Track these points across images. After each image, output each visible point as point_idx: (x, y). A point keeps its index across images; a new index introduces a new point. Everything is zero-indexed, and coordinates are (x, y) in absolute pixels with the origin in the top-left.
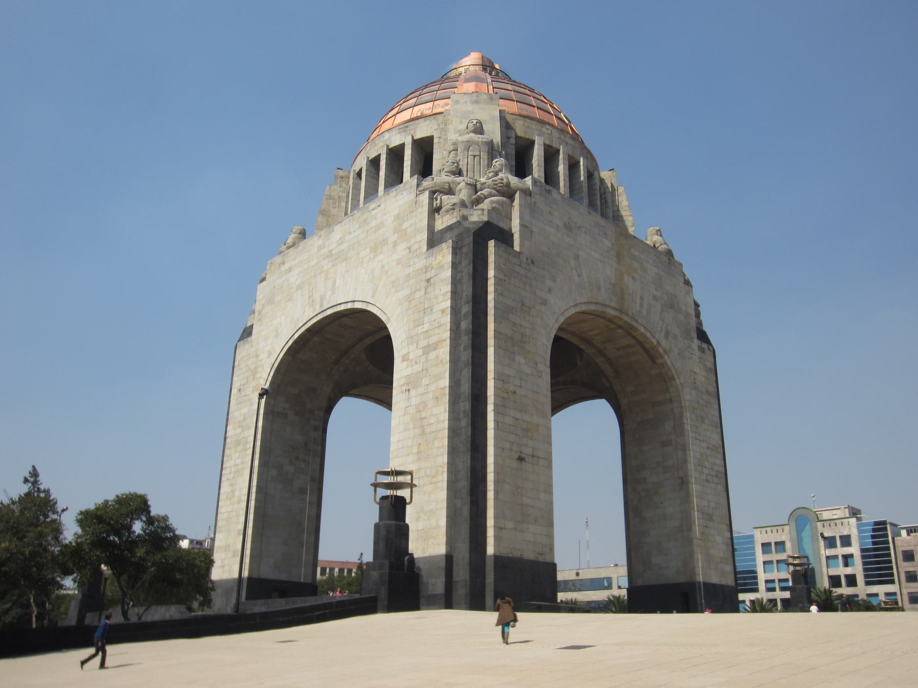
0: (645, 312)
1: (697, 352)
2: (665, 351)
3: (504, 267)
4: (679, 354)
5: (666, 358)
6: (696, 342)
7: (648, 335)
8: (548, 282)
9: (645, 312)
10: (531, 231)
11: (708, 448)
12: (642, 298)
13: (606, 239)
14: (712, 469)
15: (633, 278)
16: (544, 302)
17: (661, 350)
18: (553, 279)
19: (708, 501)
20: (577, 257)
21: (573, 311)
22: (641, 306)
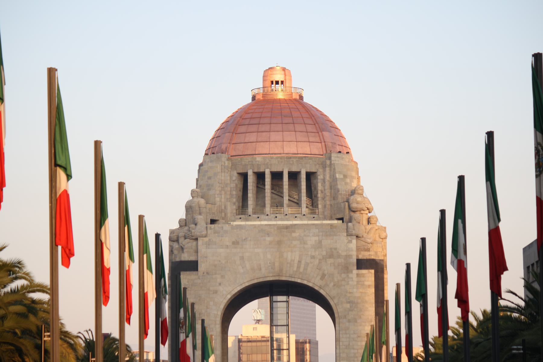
0: (301, 270)
1: (355, 279)
2: (320, 288)
3: (187, 283)
4: (334, 285)
5: (322, 291)
6: (355, 271)
7: (305, 282)
8: (219, 280)
9: (301, 270)
10: (206, 257)
12: (300, 262)
13: (269, 236)
15: (292, 252)
16: (216, 292)
17: (316, 288)
18: (223, 277)
20: (242, 258)
21: (239, 288)
22: (299, 267)
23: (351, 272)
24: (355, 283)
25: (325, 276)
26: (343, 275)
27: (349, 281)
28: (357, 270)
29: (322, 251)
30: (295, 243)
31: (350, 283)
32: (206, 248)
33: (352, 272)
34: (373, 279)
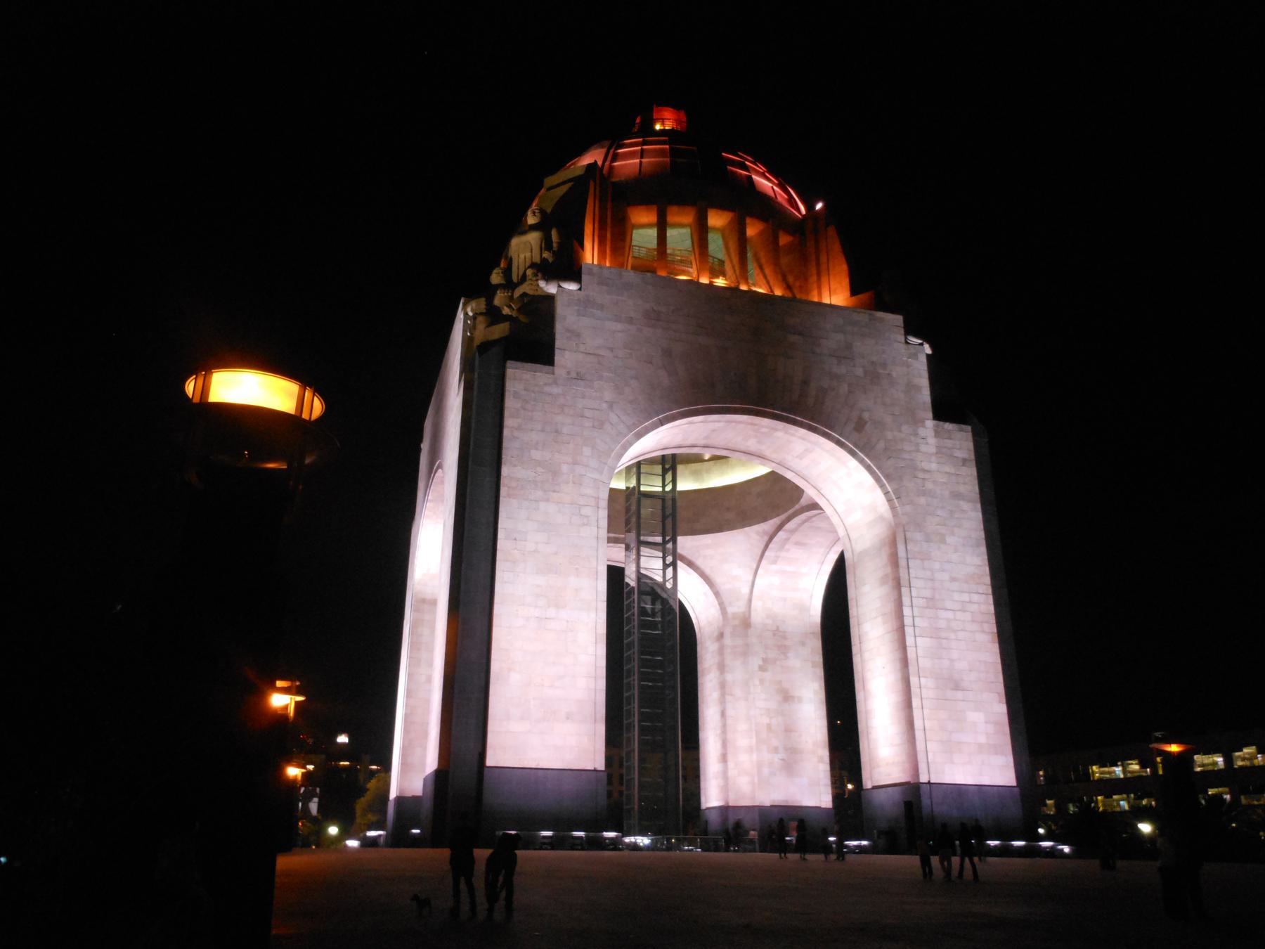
1: (932, 441)
4: (886, 449)
6: (930, 423)
10: (578, 335)
11: (953, 579)
14: (963, 610)
19: (952, 660)
23: (921, 422)
24: (933, 450)
25: (866, 423)
26: (904, 428)
27: (917, 444)
28: (935, 422)
29: (854, 366)
30: (794, 338)
31: (923, 448)
32: (579, 315)
33: (924, 427)
34: (971, 445)
